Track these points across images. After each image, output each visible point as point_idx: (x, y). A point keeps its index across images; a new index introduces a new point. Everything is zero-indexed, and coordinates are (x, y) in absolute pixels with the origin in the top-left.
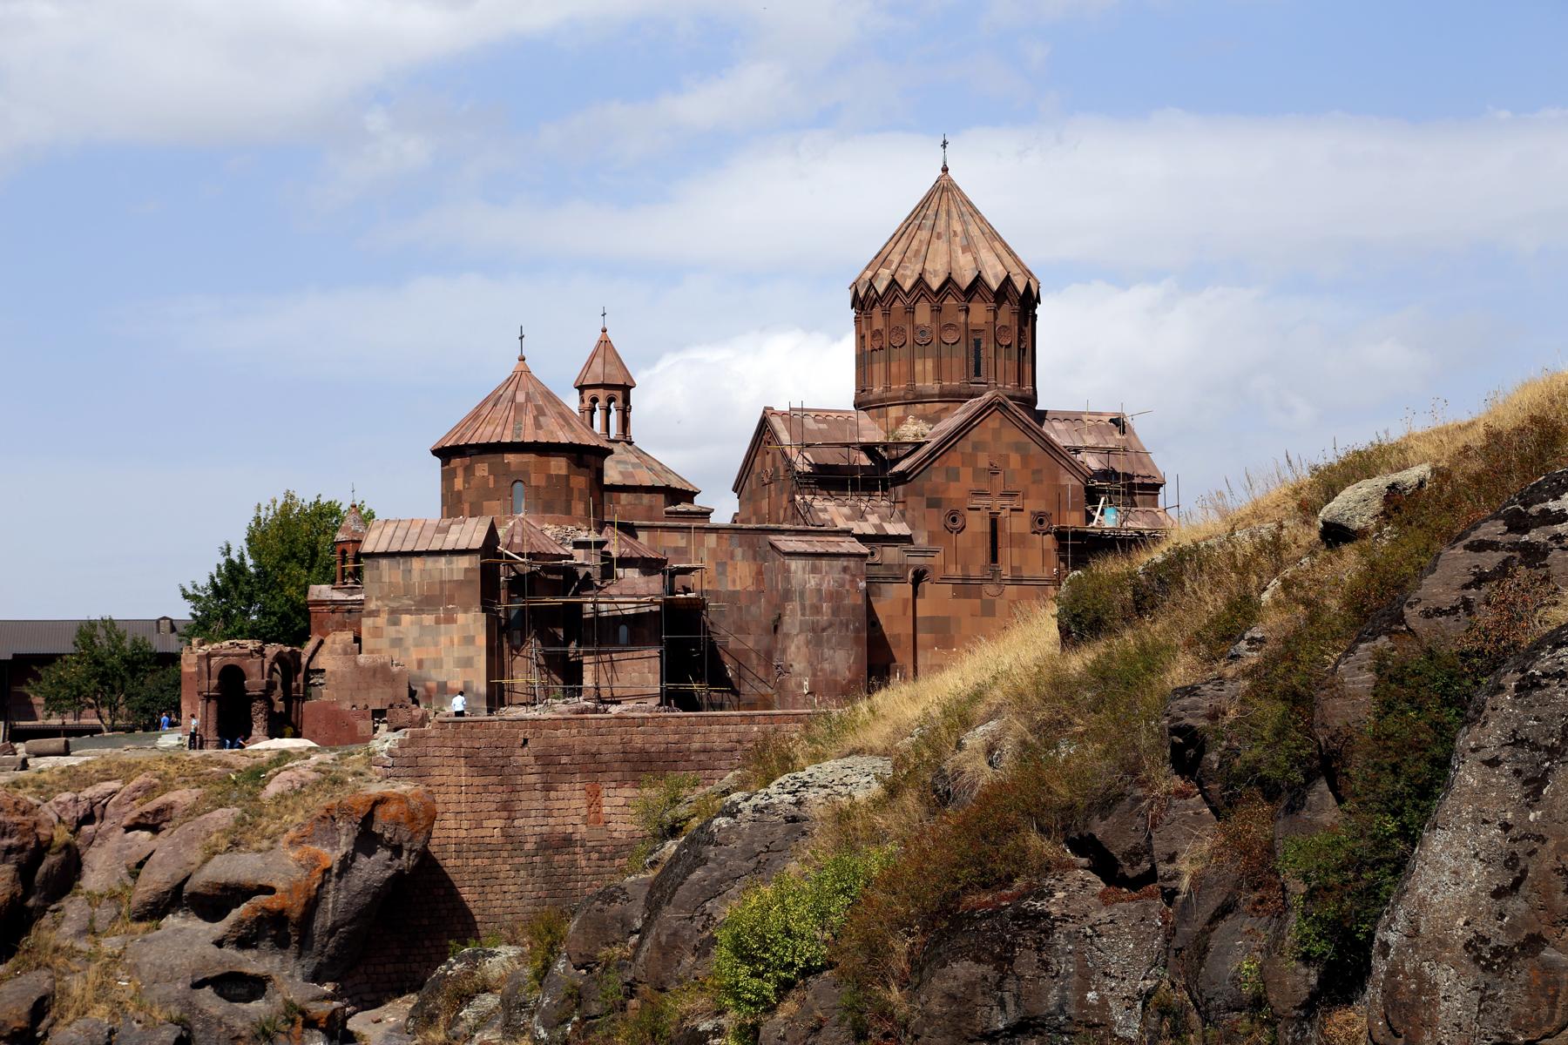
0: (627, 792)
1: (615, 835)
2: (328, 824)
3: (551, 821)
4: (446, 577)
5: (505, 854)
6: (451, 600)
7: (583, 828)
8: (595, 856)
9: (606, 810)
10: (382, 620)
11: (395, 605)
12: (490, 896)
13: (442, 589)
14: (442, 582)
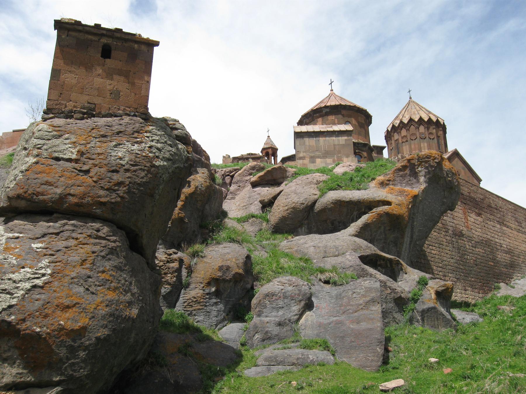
0: (473, 215)
1: (474, 236)
2: (407, 171)
3: (455, 221)
4: (336, 143)
5: (443, 233)
6: (339, 152)
7: (465, 229)
8: (470, 244)
9: (469, 223)
10: (307, 161)
11: (312, 155)
12: (442, 254)
13: (335, 148)
14: (334, 145)
